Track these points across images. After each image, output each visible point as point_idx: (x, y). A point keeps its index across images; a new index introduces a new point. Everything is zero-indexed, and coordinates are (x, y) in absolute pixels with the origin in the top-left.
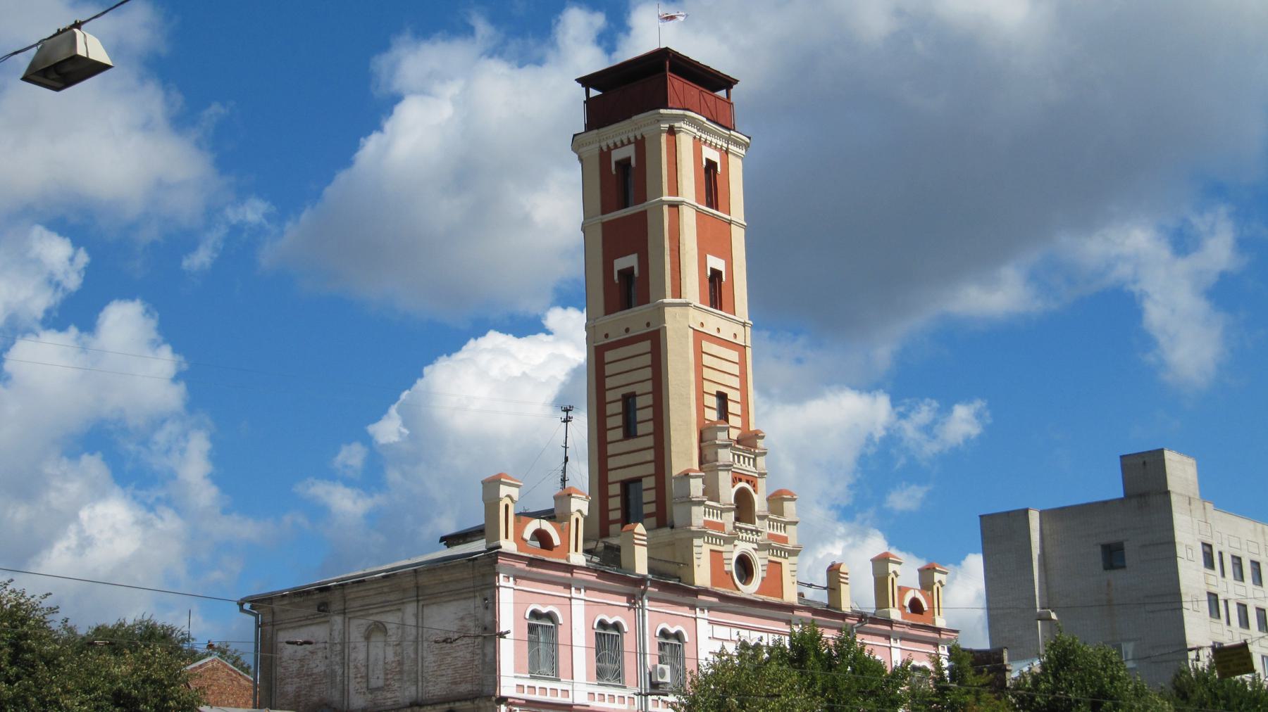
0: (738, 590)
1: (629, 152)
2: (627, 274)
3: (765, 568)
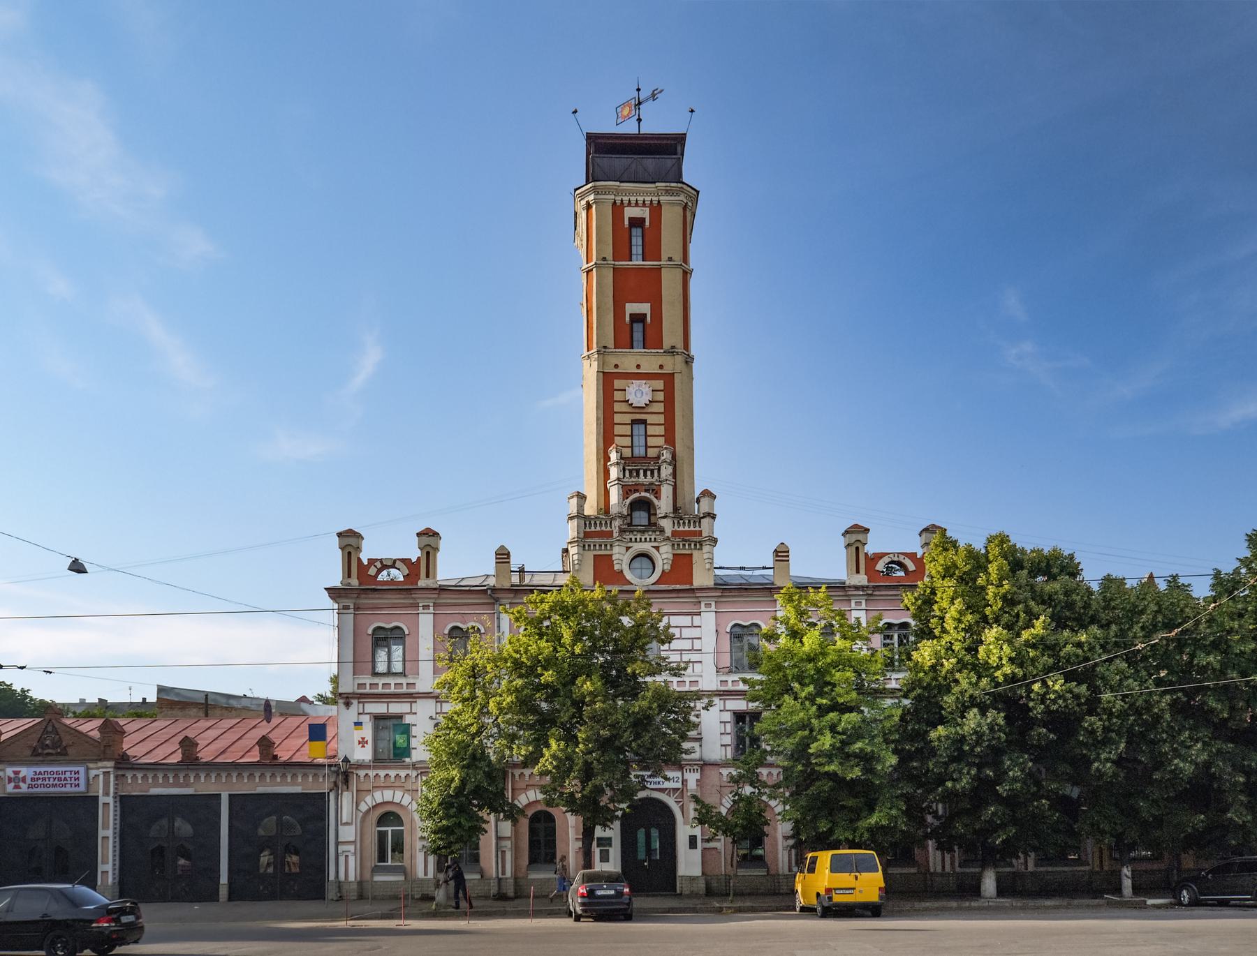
0: (632, 584)
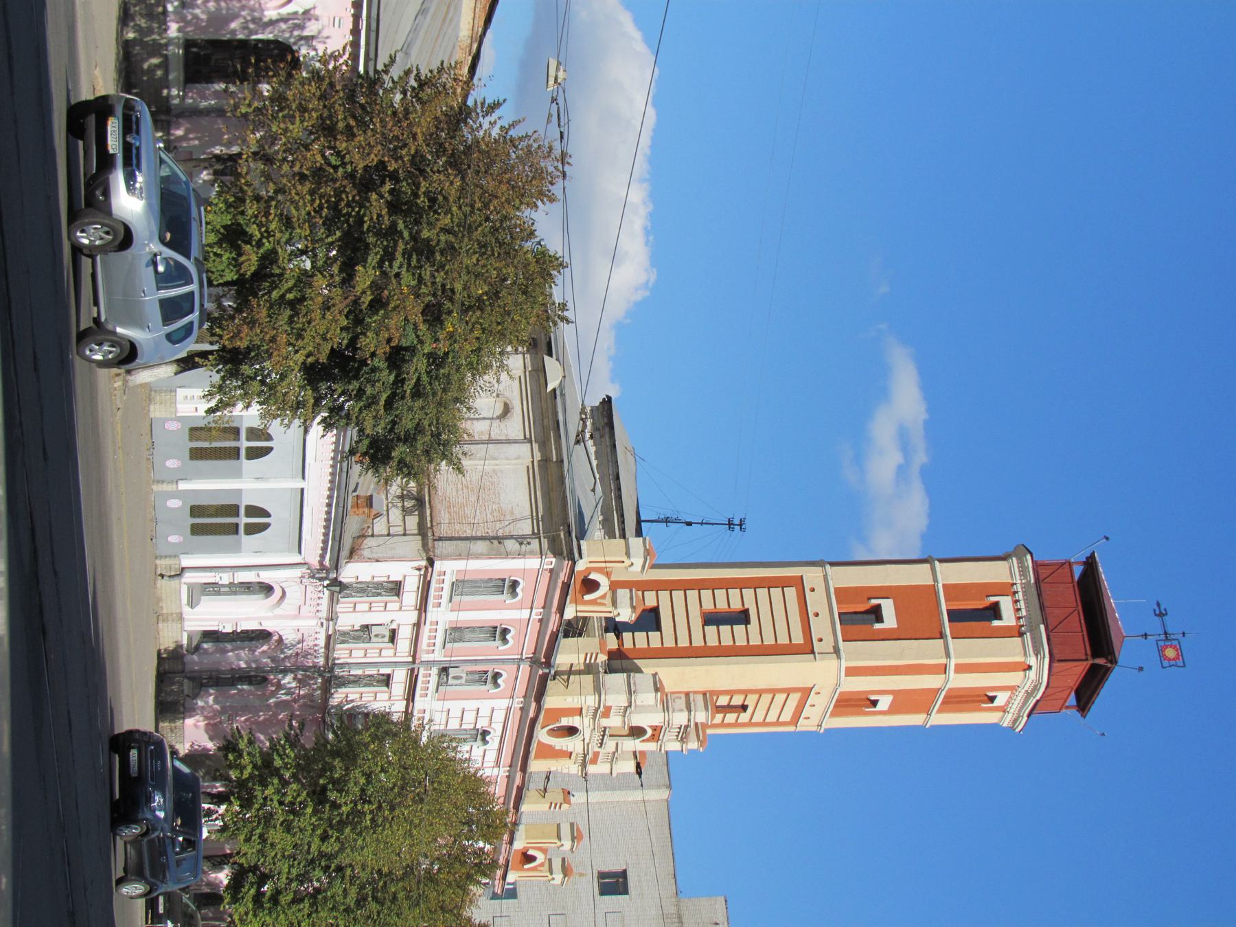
0: (542, 728)
1: (1008, 618)
2: (876, 613)
3: (564, 748)
